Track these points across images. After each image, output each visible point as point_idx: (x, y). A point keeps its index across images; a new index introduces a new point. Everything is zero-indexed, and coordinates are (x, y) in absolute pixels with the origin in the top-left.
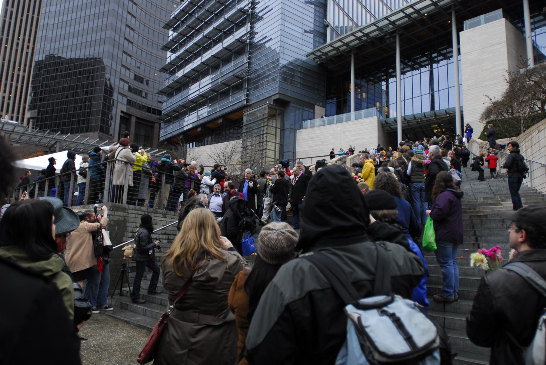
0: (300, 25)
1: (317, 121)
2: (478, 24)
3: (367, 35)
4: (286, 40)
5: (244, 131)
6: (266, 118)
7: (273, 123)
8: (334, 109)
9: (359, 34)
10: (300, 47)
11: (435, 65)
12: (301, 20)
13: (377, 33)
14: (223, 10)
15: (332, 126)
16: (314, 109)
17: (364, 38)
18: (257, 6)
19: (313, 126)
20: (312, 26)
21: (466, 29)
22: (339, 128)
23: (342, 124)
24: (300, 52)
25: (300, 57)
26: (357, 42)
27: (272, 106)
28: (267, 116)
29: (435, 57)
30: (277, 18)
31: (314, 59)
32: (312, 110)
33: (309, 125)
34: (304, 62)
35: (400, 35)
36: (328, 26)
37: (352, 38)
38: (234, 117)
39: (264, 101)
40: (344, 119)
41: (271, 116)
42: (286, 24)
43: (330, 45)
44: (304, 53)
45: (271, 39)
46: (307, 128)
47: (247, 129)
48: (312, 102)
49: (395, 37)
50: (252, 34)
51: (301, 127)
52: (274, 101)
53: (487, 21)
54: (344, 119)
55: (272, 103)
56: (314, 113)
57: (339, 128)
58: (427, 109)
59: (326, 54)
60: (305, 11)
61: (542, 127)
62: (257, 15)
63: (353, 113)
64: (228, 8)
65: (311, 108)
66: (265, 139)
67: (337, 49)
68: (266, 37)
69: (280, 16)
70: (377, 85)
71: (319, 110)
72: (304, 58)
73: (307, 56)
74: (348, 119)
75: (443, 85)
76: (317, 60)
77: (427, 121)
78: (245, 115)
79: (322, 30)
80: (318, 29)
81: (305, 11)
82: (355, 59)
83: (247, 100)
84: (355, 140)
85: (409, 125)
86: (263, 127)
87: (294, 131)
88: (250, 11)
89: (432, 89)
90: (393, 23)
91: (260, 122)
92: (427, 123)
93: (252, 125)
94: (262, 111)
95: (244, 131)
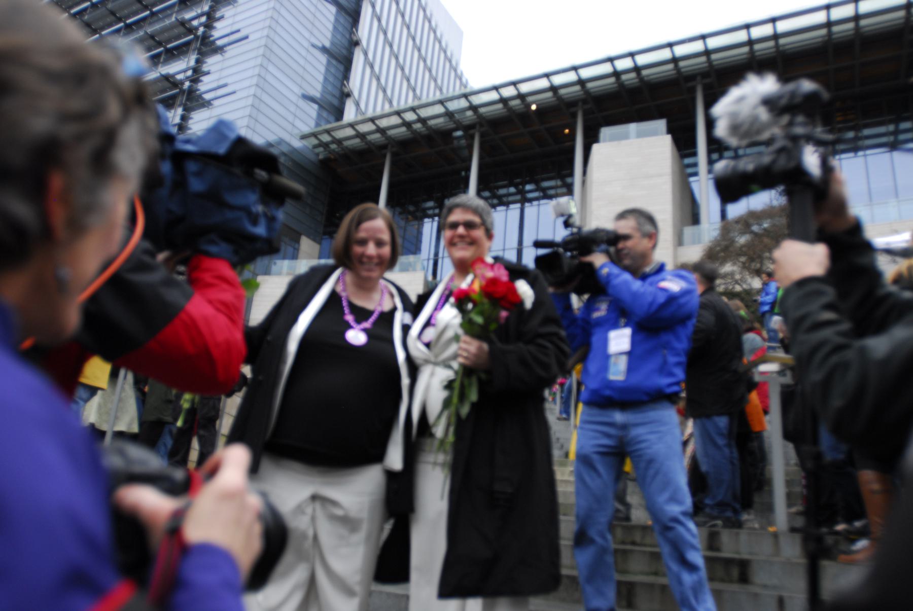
0: (299, 80)
2: (626, 137)
3: (423, 121)
4: (265, 98)
9: (410, 117)
10: (291, 118)
11: (527, 204)
12: (300, 71)
13: (441, 120)
14: (144, 19)
16: (298, 241)
17: (418, 126)
18: (218, 25)
20: (319, 87)
21: (605, 141)
24: (289, 127)
25: (287, 137)
26: (404, 129)
30: (261, 25)
31: (315, 147)
34: (294, 150)
35: (482, 136)
36: (348, 95)
37: (395, 120)
42: (271, 68)
43: (351, 125)
44: (296, 131)
45: (234, 92)
49: (472, 137)
50: (197, 73)
53: (640, 135)
59: (339, 142)
60: (310, 58)
62: (213, 42)
64: (155, 18)
67: (362, 136)
68: (225, 85)
69: (261, 51)
70: (416, 223)
72: (297, 144)
73: (304, 137)
76: (321, 149)
79: (336, 102)
80: (330, 98)
81: (310, 58)
82: (393, 164)
88: (202, 29)
90: (474, 108)
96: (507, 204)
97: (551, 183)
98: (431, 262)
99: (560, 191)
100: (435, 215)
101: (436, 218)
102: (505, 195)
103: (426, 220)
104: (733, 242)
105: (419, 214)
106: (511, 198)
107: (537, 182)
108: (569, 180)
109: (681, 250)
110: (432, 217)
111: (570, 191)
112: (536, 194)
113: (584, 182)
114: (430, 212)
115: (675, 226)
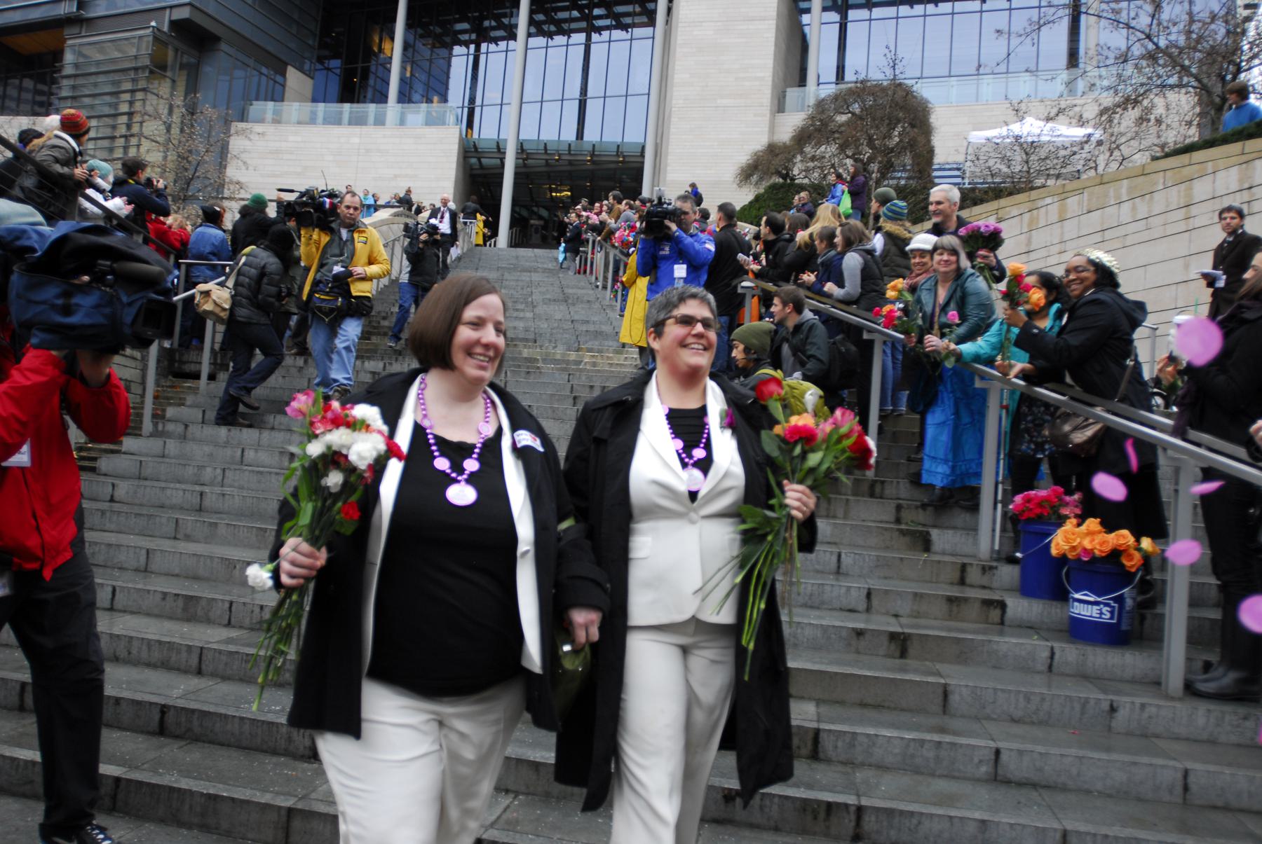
1: (294, 108)
5: (65, 93)
6: (143, 68)
7: (164, 88)
8: (334, 87)
11: (595, 37)
15: (335, 131)
16: (284, 74)
19: (277, 121)
22: (356, 140)
23: (364, 129)
27: (164, 38)
28: (147, 62)
29: (600, 17)
32: (279, 78)
33: (269, 116)
38: (25, 44)
39: (146, 16)
40: (371, 119)
41: (158, 68)
46: (261, 121)
47: (74, 87)
48: (283, 58)
51: (243, 117)
52: (174, 24)
54: (371, 119)
55: (166, 29)
56: (284, 86)
57: (356, 140)
58: (569, 135)
61: (1015, 212)
63: (392, 106)
65: (277, 72)
66: (135, 129)
70: (443, 52)
71: (294, 78)
74: (380, 121)
75: (617, 87)
77: (570, 163)
78: (74, 45)
83: (81, 6)
84: (396, 176)
85: (525, 166)
86: (133, 91)
87: (227, 123)
89: (584, 90)
91: (116, 77)
92: (568, 168)
93: (101, 79)
94: (135, 45)
95: (64, 93)
96: (567, 33)
97: (629, 8)
98: (466, 110)
99: (637, 20)
100: (472, 42)
101: (472, 47)
102: (565, 21)
103: (458, 50)
104: (831, 119)
105: (448, 39)
106: (574, 26)
107: (608, 7)
108: (651, 6)
109: (780, 117)
110: (466, 44)
111: (652, 22)
112: (607, 22)
113: (669, 10)
114: (465, 37)
115: (774, 86)
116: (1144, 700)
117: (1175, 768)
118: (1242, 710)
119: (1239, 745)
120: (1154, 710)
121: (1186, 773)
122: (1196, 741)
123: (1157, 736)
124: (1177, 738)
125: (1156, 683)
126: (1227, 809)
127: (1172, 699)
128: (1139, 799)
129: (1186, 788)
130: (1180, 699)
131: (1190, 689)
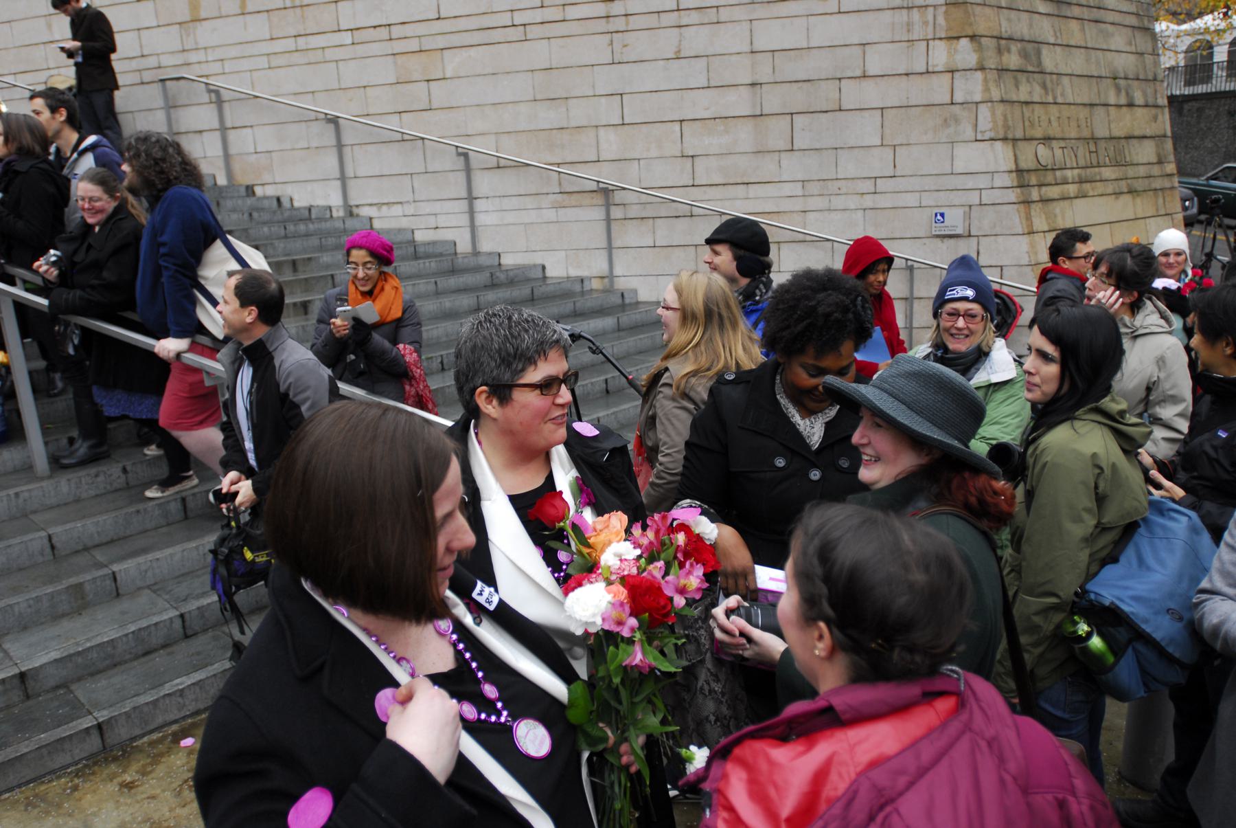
116: (17, 490)
117: (41, 538)
118: (92, 470)
119: (97, 496)
120: (26, 495)
121: (50, 538)
122: (66, 504)
123: (35, 512)
124: (51, 508)
125: (26, 470)
126: (86, 549)
127: (42, 479)
128: (20, 569)
129: (53, 547)
130: (50, 477)
131: (57, 464)
